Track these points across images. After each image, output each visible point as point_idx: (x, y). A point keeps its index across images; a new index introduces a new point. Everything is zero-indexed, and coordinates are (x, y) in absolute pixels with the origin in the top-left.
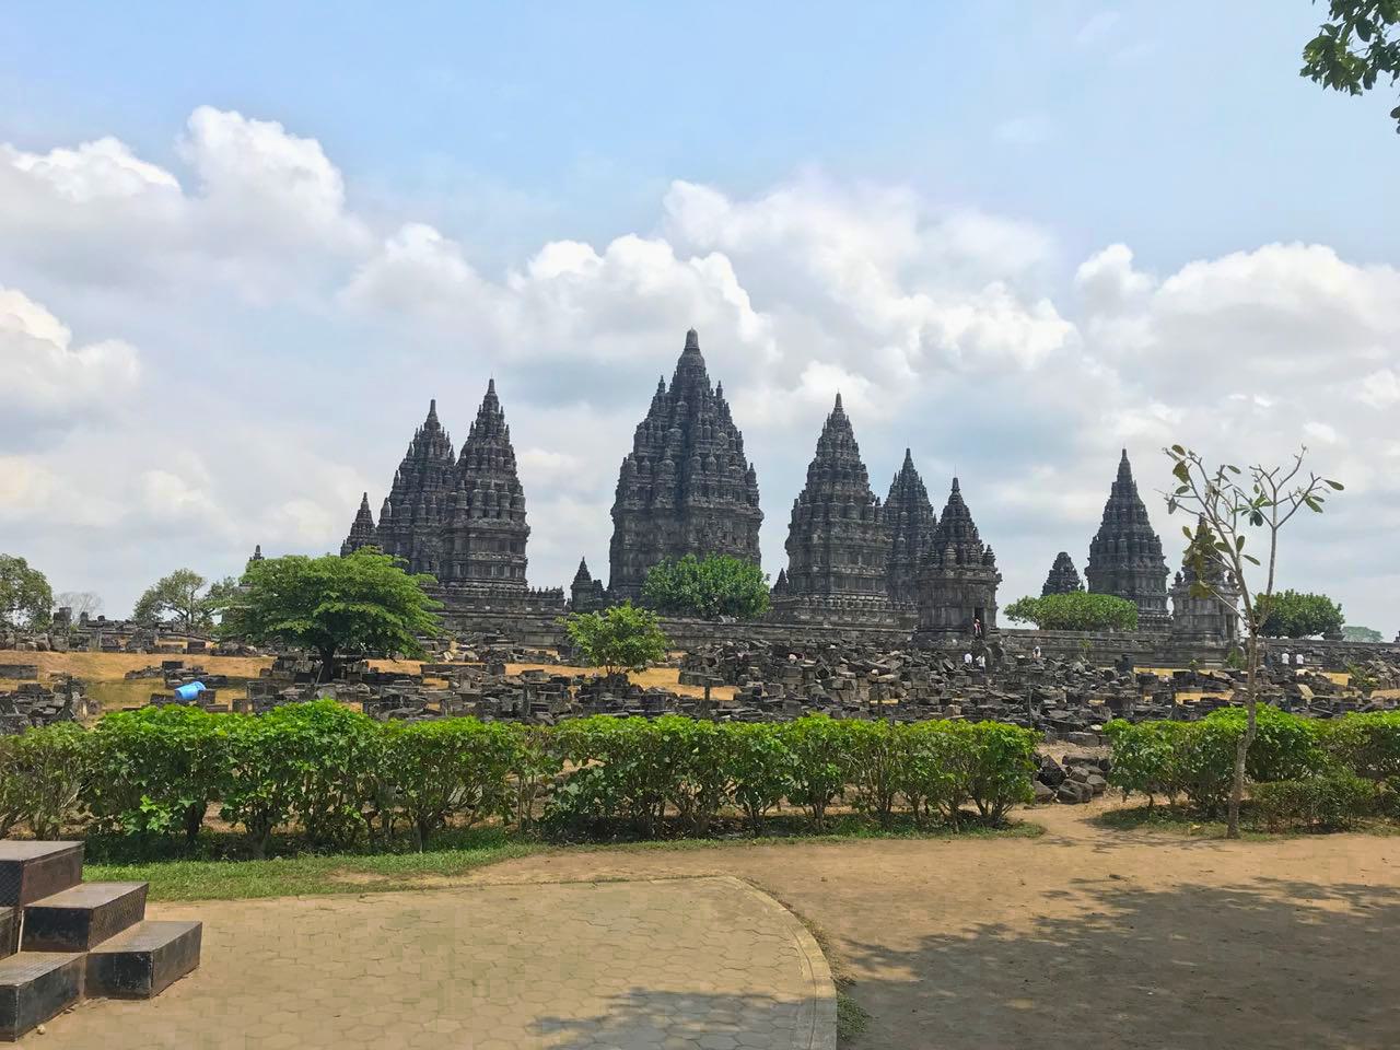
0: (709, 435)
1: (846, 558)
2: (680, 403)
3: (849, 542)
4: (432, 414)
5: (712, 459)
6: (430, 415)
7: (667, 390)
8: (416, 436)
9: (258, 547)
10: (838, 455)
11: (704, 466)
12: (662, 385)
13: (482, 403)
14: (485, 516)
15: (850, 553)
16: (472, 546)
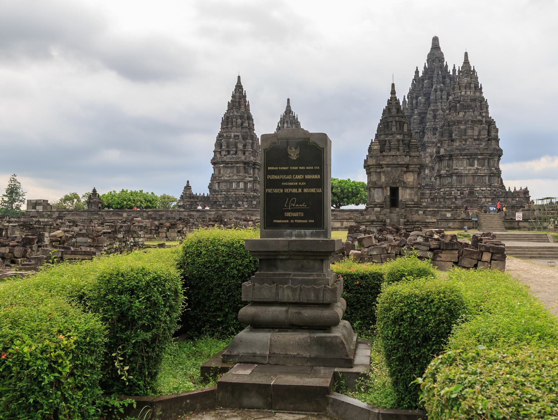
0: (439, 97)
1: (465, 162)
2: (426, 82)
3: (466, 152)
4: (288, 107)
5: (440, 112)
6: (287, 107)
7: (421, 74)
8: (281, 119)
9: (188, 182)
10: (463, 93)
11: (435, 117)
12: (417, 72)
13: (234, 90)
14: (229, 154)
15: (468, 159)
16: (222, 172)
